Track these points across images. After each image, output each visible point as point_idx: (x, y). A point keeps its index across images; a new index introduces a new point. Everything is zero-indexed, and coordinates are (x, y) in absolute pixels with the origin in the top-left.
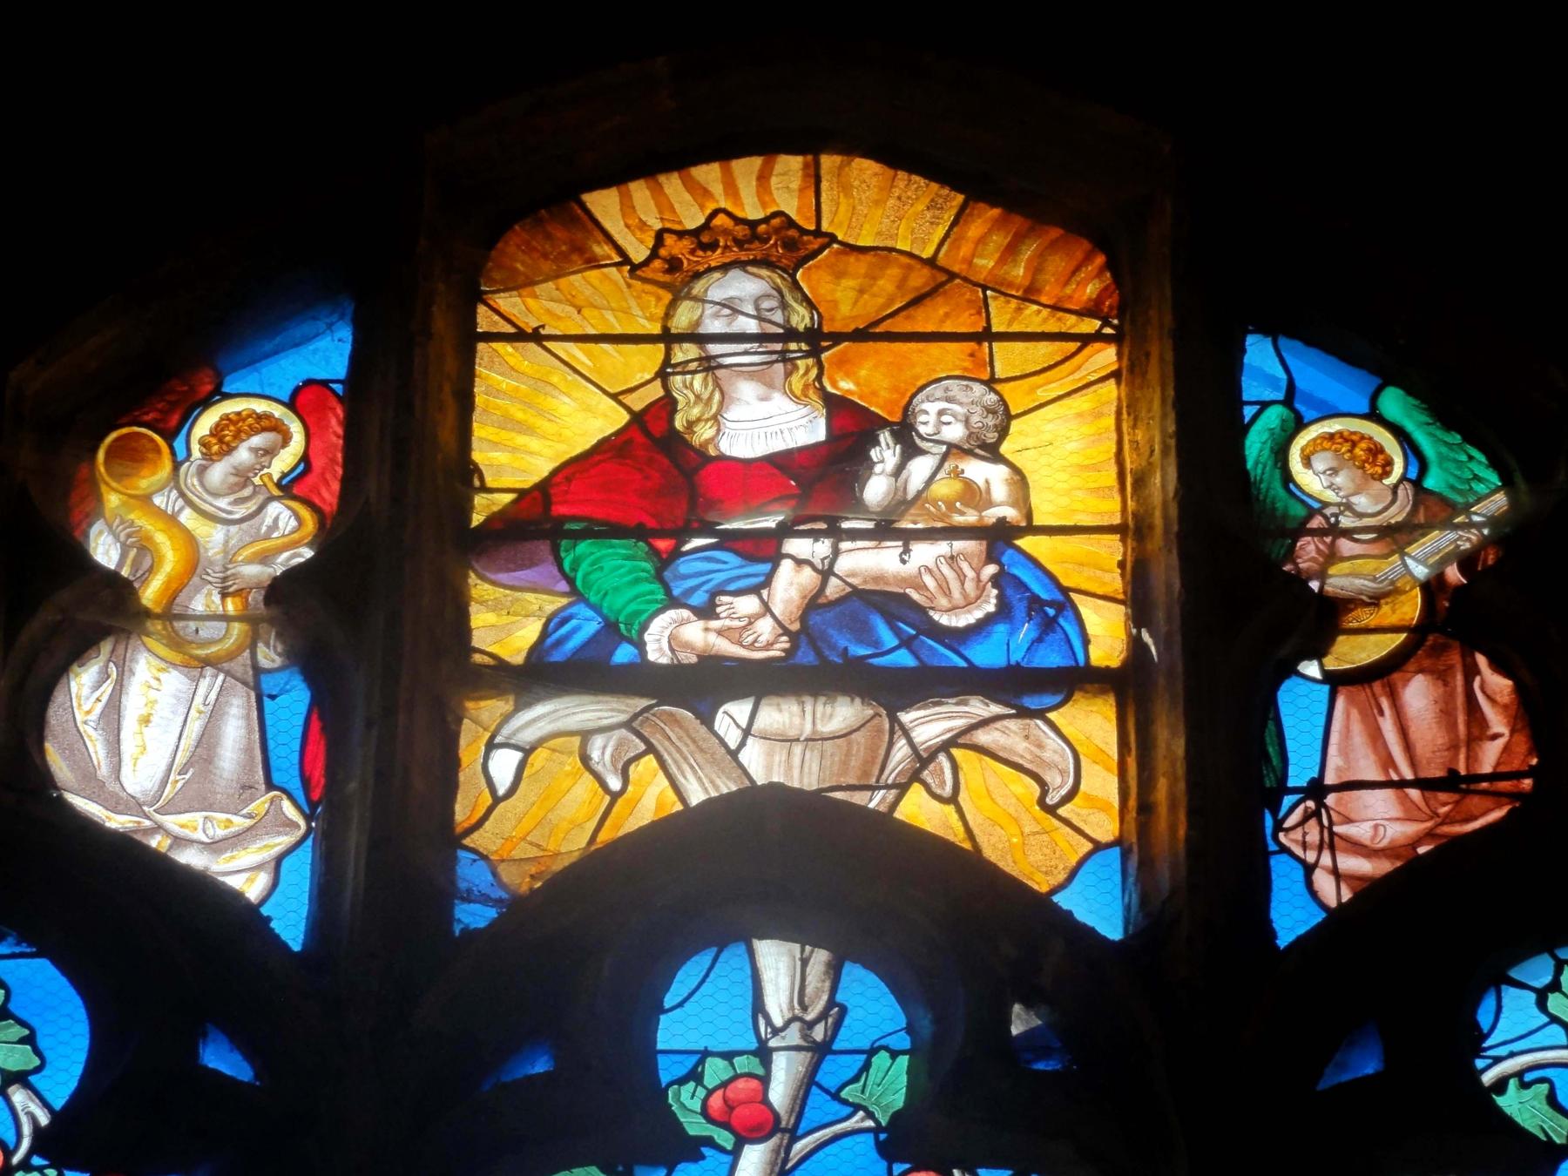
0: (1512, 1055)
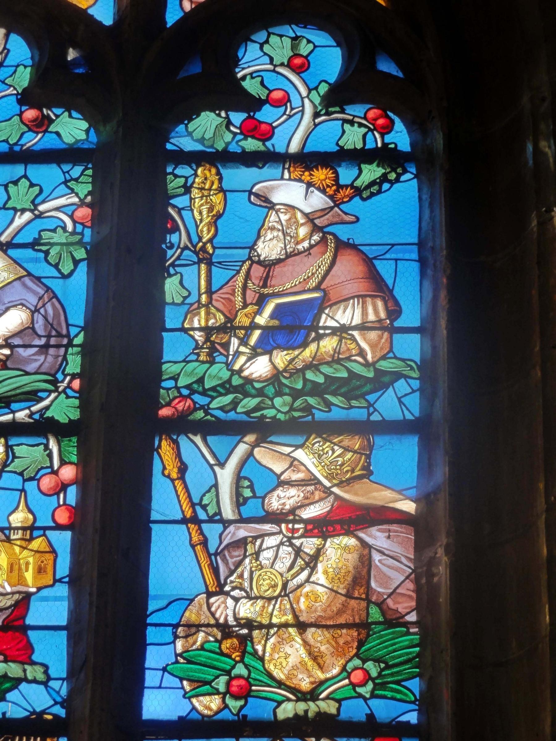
0: (249, 67)
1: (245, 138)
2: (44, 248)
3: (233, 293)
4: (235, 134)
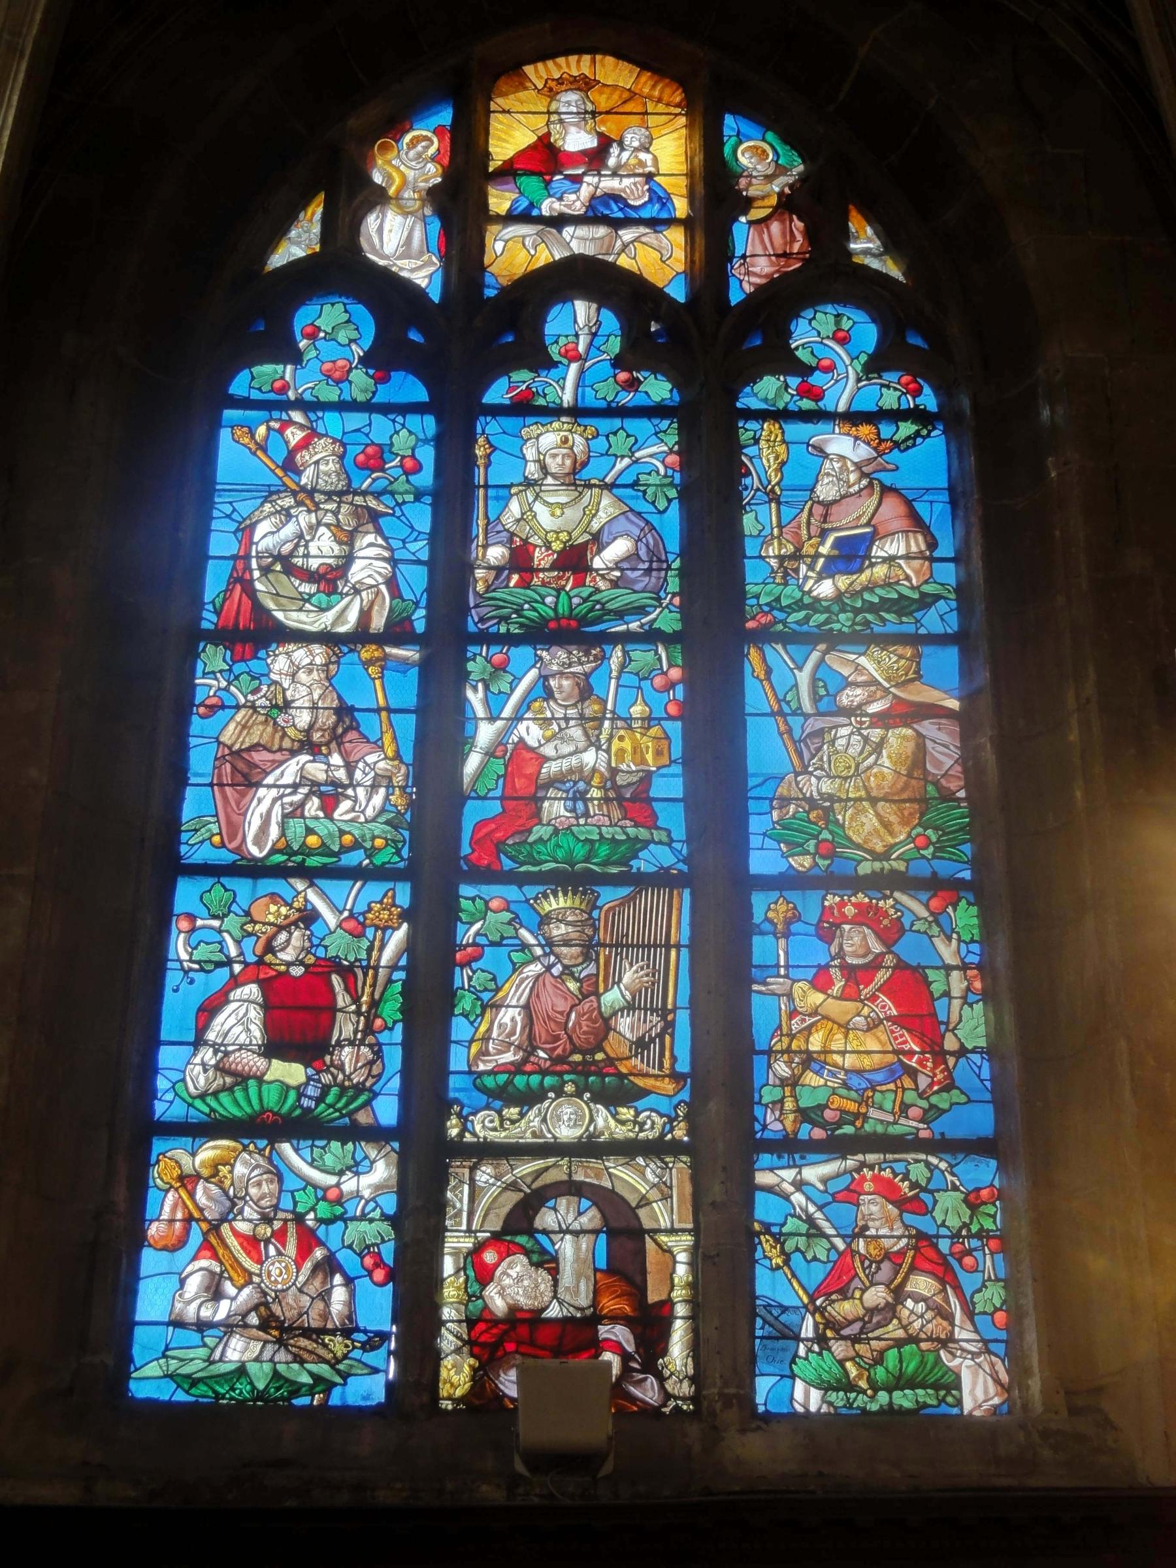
1: (801, 399)
2: (642, 488)
3: (799, 527)
4: (793, 396)
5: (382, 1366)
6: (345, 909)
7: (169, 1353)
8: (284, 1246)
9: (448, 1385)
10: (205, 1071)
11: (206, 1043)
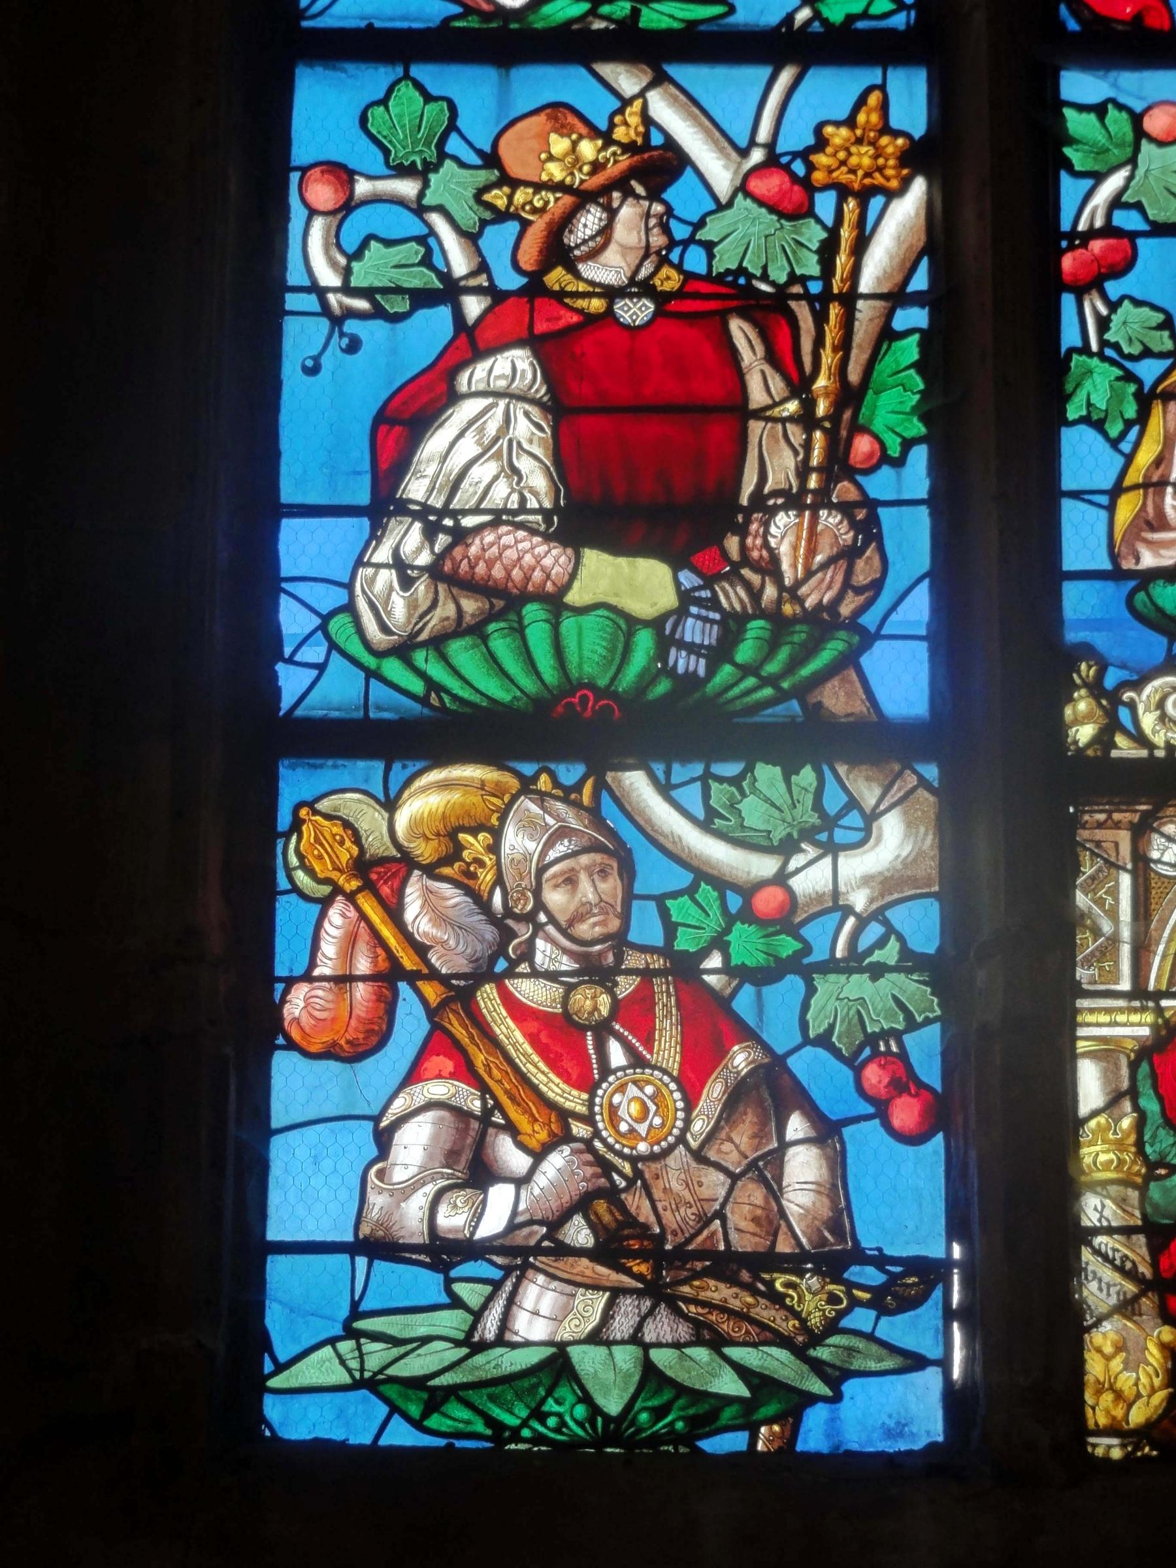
5: (933, 1351)
6: (752, 143)
7: (361, 1325)
8: (649, 1043)
9: (1107, 1398)
10: (406, 582)
11: (402, 508)
